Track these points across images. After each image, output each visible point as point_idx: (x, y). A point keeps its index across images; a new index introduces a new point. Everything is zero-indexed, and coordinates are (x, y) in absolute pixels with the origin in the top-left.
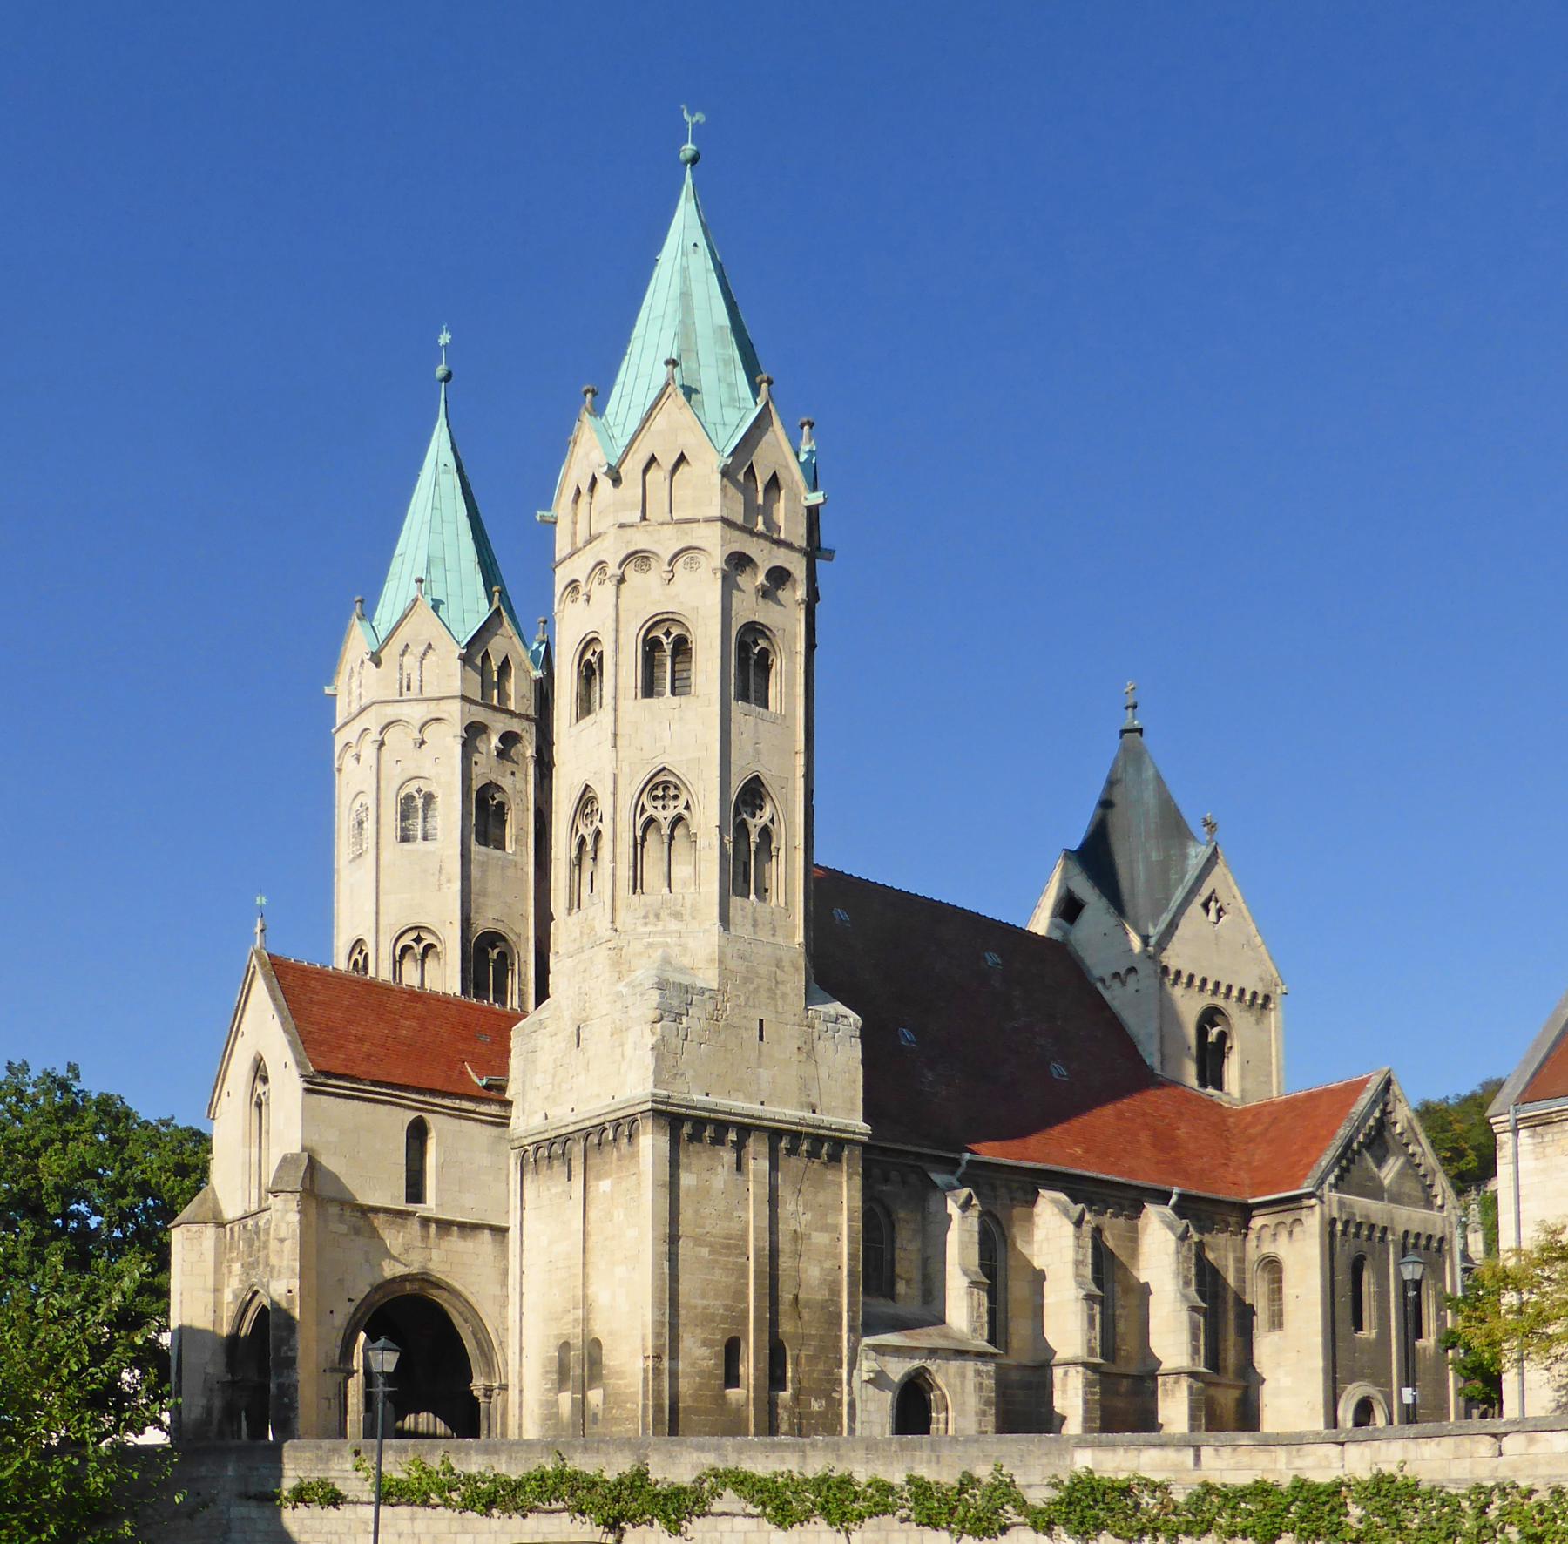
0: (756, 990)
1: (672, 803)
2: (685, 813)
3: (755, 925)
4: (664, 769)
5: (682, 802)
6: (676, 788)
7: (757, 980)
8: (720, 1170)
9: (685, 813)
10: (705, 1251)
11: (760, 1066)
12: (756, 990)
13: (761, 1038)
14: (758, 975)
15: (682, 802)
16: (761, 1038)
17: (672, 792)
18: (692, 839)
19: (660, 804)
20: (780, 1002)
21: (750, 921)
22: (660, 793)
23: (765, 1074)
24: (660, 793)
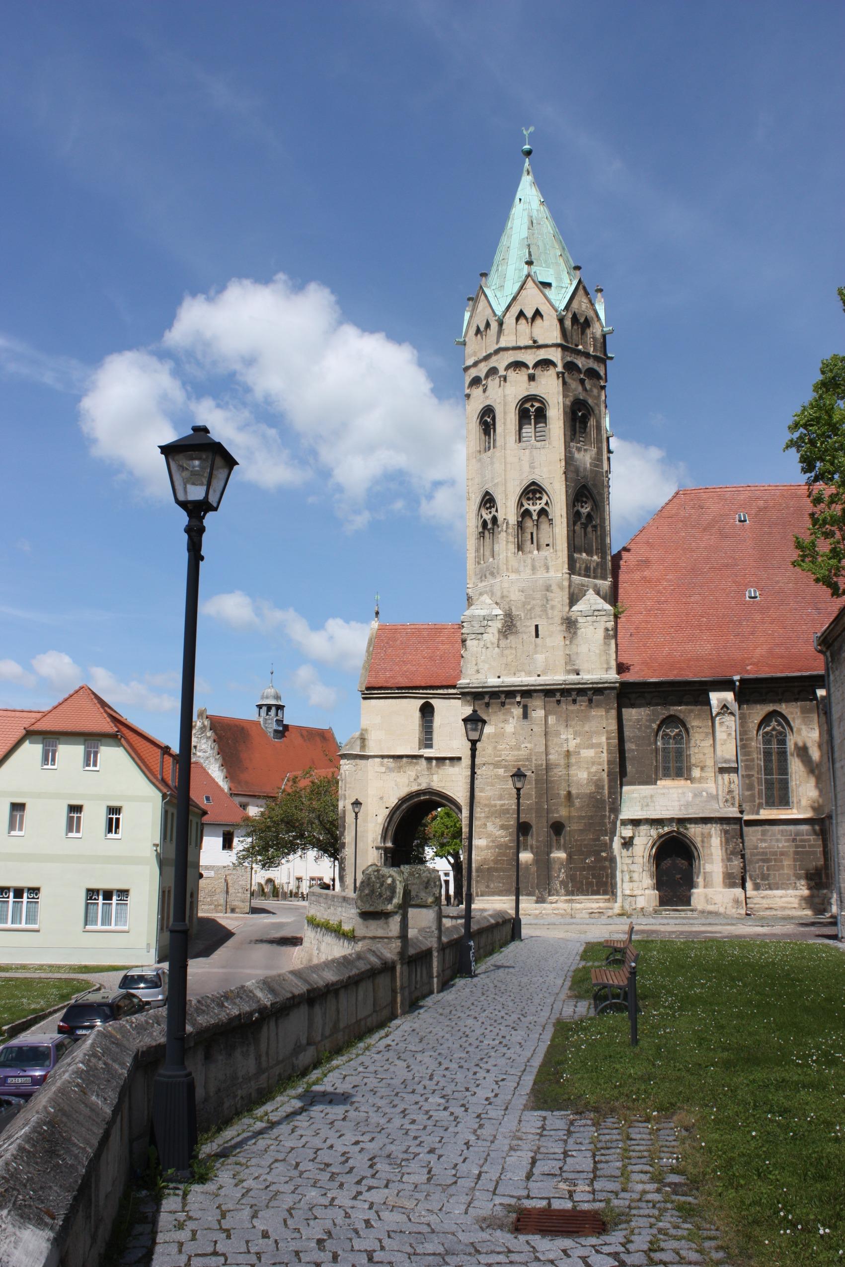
0: (532, 609)
3: (534, 568)
7: (534, 602)
8: (511, 720)
10: (501, 771)
12: (532, 609)
13: (537, 636)
16: (537, 636)
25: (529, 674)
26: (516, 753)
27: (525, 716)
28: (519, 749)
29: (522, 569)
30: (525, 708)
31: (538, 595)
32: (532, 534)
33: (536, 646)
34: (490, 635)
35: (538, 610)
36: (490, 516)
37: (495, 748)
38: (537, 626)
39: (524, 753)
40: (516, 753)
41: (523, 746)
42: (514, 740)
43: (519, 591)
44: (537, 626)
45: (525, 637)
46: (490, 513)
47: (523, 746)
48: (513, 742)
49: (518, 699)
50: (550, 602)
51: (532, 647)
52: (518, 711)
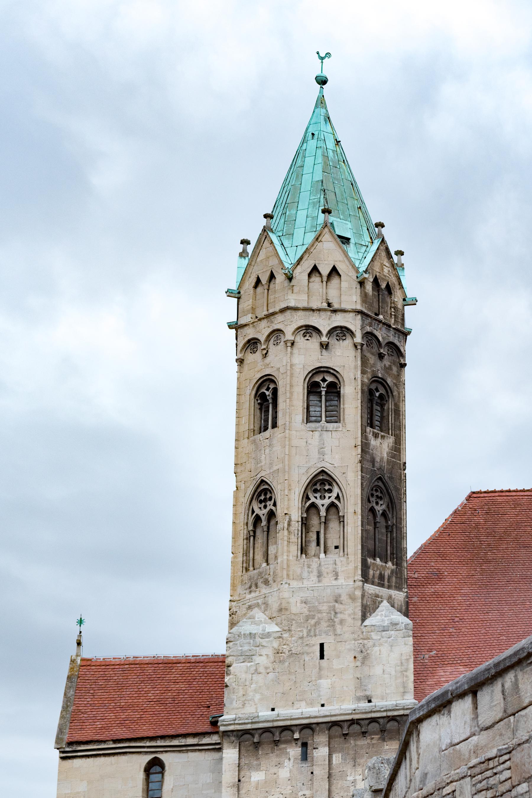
1: (327, 495)
2: (336, 502)
3: (320, 575)
4: (323, 471)
5: (334, 495)
6: (330, 484)
7: (319, 615)
9: (336, 502)
11: (320, 677)
13: (322, 657)
14: (320, 612)
15: (334, 495)
16: (322, 657)
17: (327, 487)
18: (341, 520)
19: (318, 495)
21: (315, 573)
22: (318, 487)
23: (325, 683)
24: (318, 487)
25: (311, 704)
27: (305, 757)
29: (305, 575)
30: (305, 745)
31: (324, 608)
32: (318, 533)
33: (320, 669)
36: (265, 511)
38: (322, 645)
42: (289, 787)
43: (302, 602)
44: (322, 645)
45: (307, 658)
46: (265, 507)
49: (297, 736)
50: (339, 615)
51: (315, 671)
52: (295, 751)
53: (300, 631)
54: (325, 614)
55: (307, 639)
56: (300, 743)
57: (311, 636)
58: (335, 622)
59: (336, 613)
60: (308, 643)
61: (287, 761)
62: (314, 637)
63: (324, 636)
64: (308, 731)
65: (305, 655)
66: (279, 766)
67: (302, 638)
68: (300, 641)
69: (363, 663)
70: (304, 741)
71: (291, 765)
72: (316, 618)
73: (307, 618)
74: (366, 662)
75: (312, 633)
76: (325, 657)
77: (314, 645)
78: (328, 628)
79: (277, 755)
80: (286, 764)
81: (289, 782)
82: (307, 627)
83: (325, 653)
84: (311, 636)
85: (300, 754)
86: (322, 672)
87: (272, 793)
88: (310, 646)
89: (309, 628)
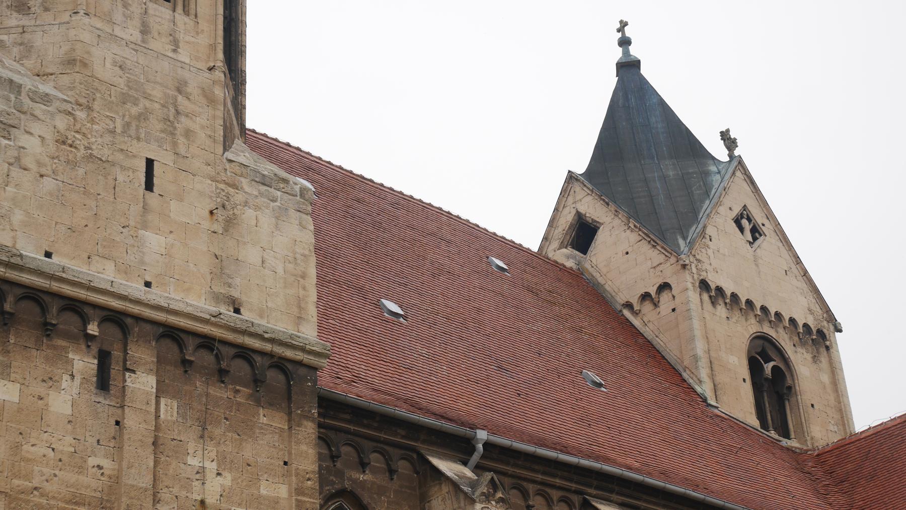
0: (142, 117)
12: (142, 117)
13: (149, 185)
14: (147, 97)
16: (149, 185)
20: (181, 140)
26: (71, 477)
27: (103, 382)
28: (81, 469)
30: (104, 359)
33: (145, 207)
34: (36, 141)
35: (155, 126)
37: (17, 447)
38: (150, 163)
39: (94, 484)
40: (71, 477)
41: (92, 461)
42: (69, 439)
44: (150, 163)
45: (120, 178)
47: (92, 461)
48: (66, 445)
50: (183, 119)
51: (135, 209)
52: (84, 363)
53: (112, 119)
54: (157, 106)
55: (122, 139)
56: (95, 350)
57: (131, 136)
58: (175, 128)
59: (178, 112)
60: (124, 147)
61: (66, 377)
62: (135, 142)
63: (154, 146)
64: (113, 330)
65: (118, 169)
66: (51, 383)
67: (113, 132)
68: (108, 138)
69: (226, 230)
70: (105, 348)
71: (75, 391)
72: (141, 105)
73: (125, 99)
74: (231, 230)
75: (132, 132)
76: (155, 189)
77: (134, 156)
78: (163, 135)
79: (47, 359)
80: (64, 385)
81: (69, 426)
82: (124, 116)
83: (155, 180)
84: (131, 136)
85: (95, 372)
86: (149, 217)
87: (33, 441)
88: (128, 156)
89: (127, 119)
